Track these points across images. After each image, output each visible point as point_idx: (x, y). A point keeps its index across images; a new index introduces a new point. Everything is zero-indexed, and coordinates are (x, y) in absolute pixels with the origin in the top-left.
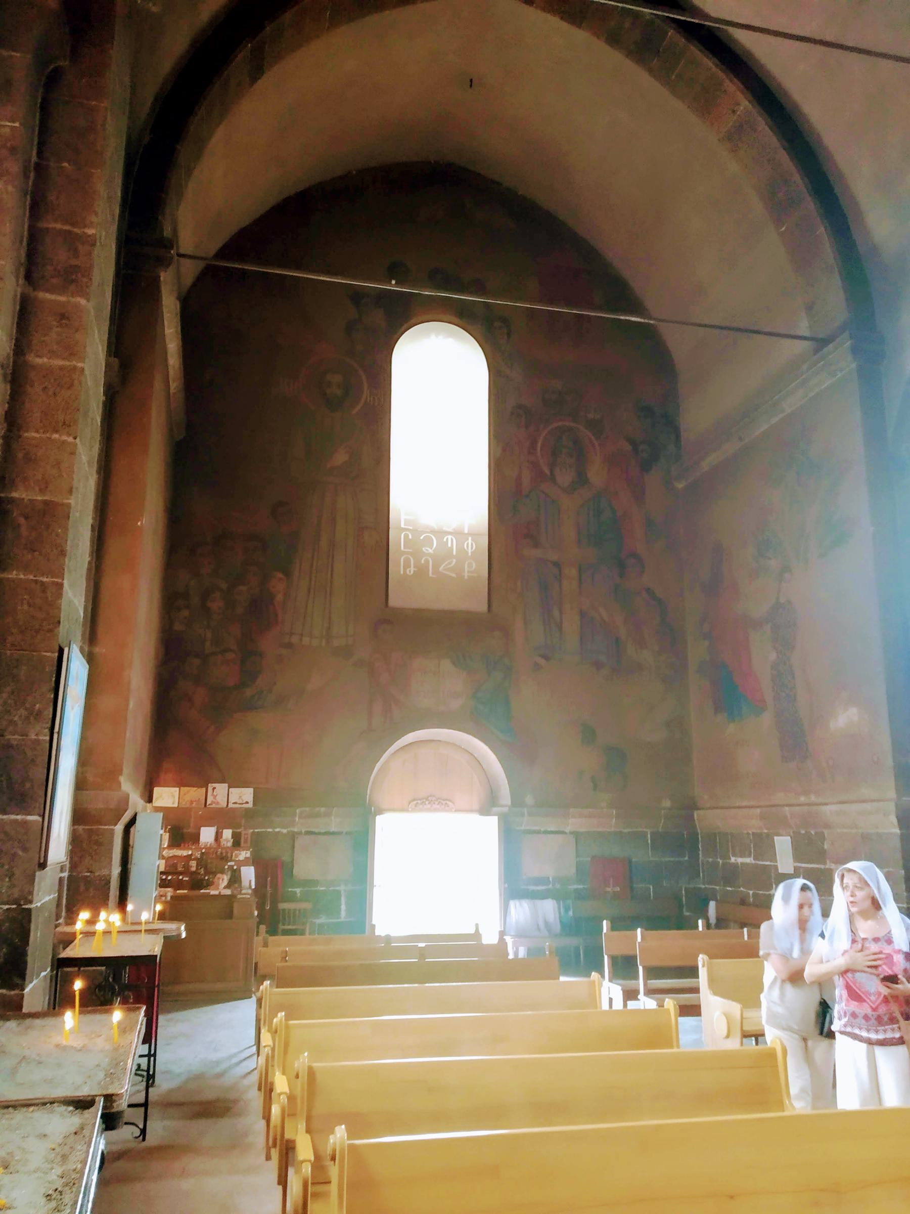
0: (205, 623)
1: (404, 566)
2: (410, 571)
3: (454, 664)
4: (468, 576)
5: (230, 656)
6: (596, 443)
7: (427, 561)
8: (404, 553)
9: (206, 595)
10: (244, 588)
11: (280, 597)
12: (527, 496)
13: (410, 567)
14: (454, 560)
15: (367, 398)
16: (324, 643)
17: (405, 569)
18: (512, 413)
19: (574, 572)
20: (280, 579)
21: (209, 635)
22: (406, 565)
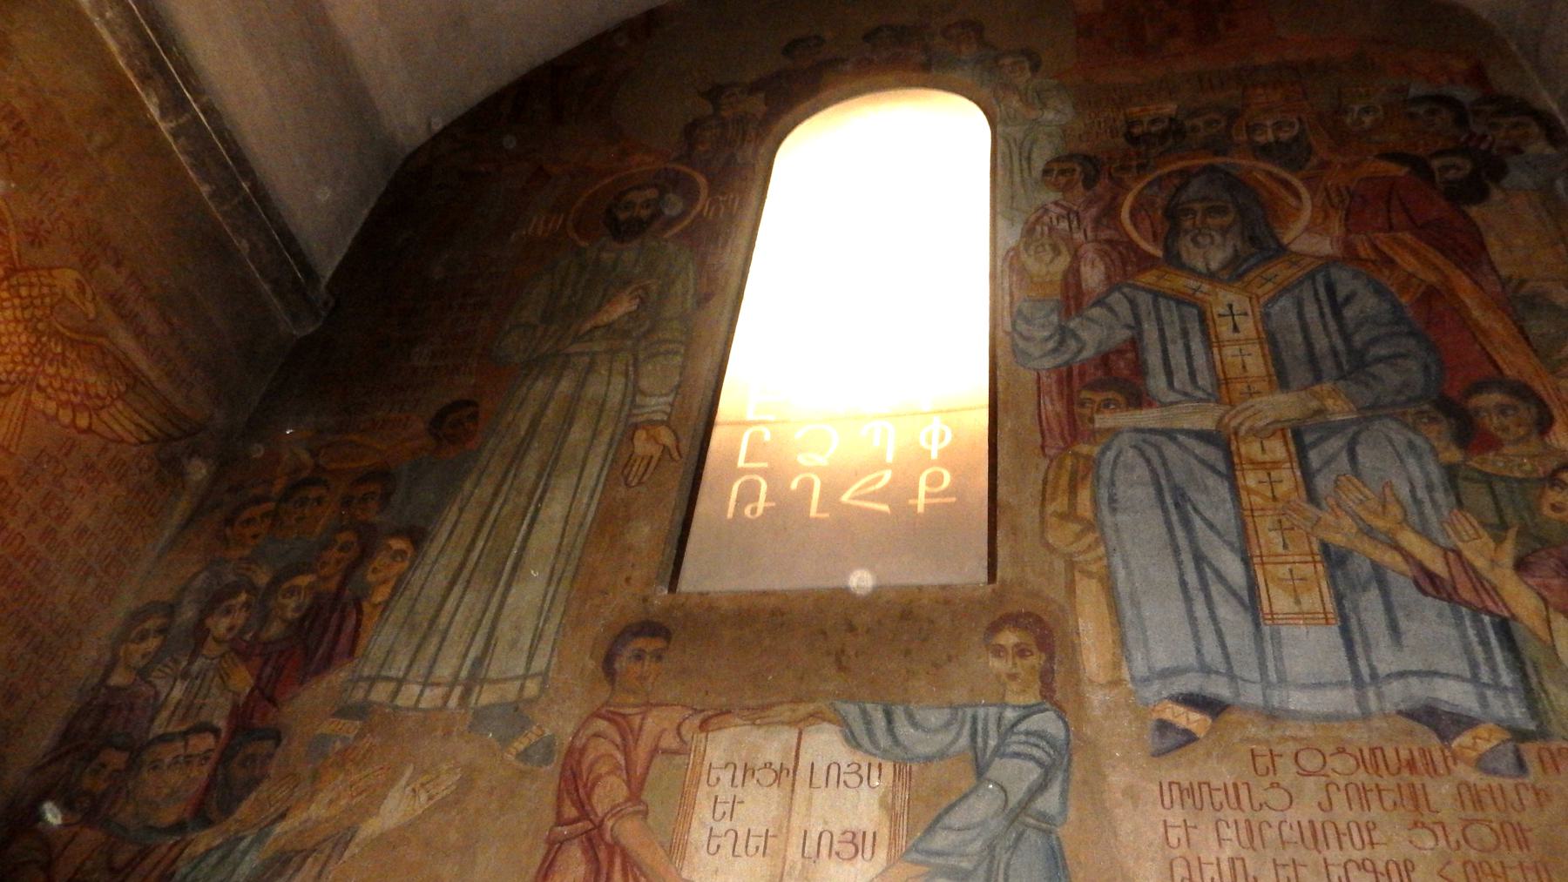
0: (184, 663)
1: (737, 501)
2: (754, 511)
3: (852, 740)
4: (927, 506)
5: (206, 742)
6: (1296, 182)
7: (807, 486)
8: (744, 471)
9: (215, 601)
10: (304, 581)
11: (380, 596)
12: (1100, 302)
13: (757, 498)
14: (887, 476)
15: (702, 211)
16: (453, 702)
17: (741, 502)
18: (1046, 172)
19: (1278, 449)
20: (402, 553)
21: (177, 693)
22: (749, 494)
